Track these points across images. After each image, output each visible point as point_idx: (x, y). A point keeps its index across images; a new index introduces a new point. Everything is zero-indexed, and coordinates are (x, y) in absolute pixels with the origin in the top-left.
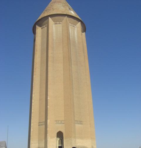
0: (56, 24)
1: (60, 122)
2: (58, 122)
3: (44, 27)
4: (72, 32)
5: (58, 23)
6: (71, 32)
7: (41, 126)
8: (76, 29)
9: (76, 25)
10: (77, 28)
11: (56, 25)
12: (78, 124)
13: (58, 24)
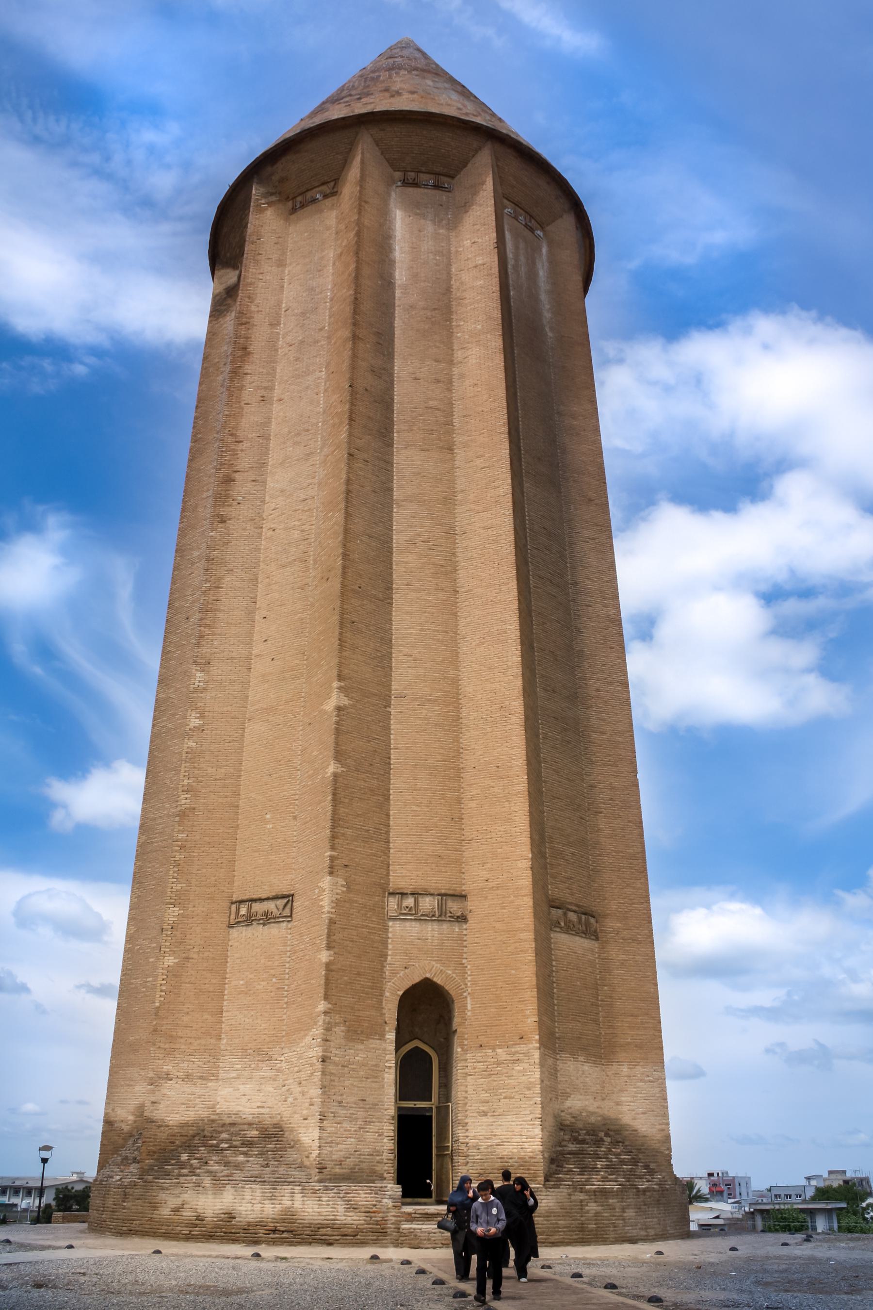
0: (415, 184)
2: (410, 901)
3: (314, 201)
4: (522, 259)
5: (423, 177)
6: (516, 259)
8: (544, 250)
9: (542, 229)
10: (550, 244)
11: (411, 190)
12: (569, 929)
13: (426, 186)
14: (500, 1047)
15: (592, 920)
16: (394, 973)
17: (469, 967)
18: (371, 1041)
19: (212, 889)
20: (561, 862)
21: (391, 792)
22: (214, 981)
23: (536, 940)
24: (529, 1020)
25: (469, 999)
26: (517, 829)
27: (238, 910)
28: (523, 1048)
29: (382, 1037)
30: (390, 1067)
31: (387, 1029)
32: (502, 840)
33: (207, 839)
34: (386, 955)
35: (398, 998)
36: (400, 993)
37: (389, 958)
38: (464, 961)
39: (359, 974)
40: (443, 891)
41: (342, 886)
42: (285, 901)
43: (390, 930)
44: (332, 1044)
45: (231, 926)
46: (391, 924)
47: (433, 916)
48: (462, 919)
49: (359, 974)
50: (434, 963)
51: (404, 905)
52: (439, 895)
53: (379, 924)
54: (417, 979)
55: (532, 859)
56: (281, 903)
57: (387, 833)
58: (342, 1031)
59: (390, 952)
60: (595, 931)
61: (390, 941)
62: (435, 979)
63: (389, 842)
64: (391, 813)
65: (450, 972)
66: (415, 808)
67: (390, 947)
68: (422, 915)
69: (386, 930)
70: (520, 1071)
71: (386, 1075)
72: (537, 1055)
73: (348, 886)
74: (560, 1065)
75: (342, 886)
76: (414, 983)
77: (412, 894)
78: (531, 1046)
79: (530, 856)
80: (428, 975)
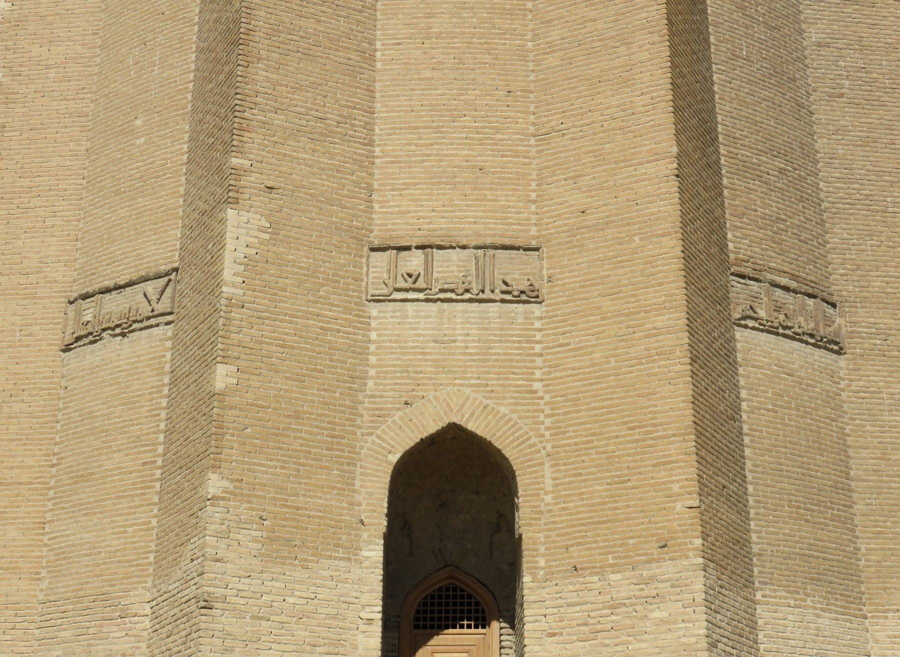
1: (450, 267)
2: (414, 261)
7: (112, 349)
14: (616, 568)
15: (830, 310)
16: (381, 416)
17: (547, 398)
18: (326, 562)
19: (33, 278)
20: (754, 185)
21: (378, 45)
22: (29, 461)
23: (692, 331)
24: (679, 506)
25: (547, 466)
26: (646, 99)
27: (79, 313)
28: (668, 569)
29: (352, 552)
30: (370, 620)
31: (365, 536)
32: (614, 124)
33: (25, 182)
34: (363, 378)
35: (390, 470)
36: (394, 458)
37: (370, 383)
38: (537, 386)
39: (297, 416)
40: (489, 241)
41: (261, 229)
42: (162, 281)
43: (374, 324)
44: (229, 566)
45: (67, 349)
46: (374, 310)
47: (467, 291)
48: (529, 296)
49: (297, 416)
50: (468, 391)
51: (403, 270)
52: (477, 247)
53: (347, 310)
54: (432, 428)
55: (679, 156)
56: (151, 288)
57: (369, 126)
58: (256, 540)
59: (372, 372)
60: (837, 333)
61: (372, 347)
62: (471, 427)
63: (371, 143)
64: (378, 86)
65: (503, 410)
66: (428, 74)
67: (373, 359)
68: (442, 291)
69: (364, 323)
70: (663, 621)
71: (360, 638)
72: (698, 584)
73: (274, 229)
74: (763, 613)
75: (261, 229)
76: (425, 435)
77: (417, 247)
78: (685, 563)
79: (675, 149)
80: (456, 420)
